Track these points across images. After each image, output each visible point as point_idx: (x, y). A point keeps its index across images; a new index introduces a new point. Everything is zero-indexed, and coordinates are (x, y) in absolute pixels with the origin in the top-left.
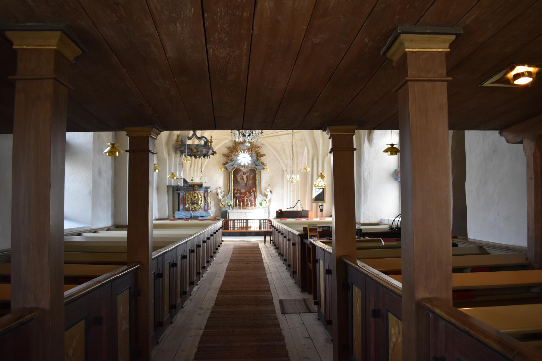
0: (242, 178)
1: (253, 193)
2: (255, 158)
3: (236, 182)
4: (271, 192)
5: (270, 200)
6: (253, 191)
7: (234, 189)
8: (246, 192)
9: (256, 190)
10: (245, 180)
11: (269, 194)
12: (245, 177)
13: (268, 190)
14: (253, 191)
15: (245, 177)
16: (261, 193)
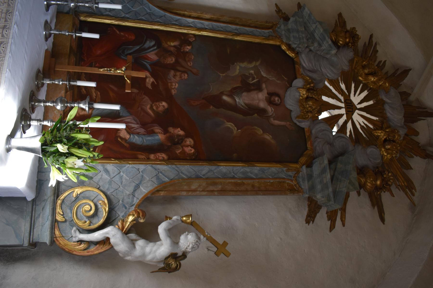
0: (246, 86)
1: (160, 137)
2: (362, 161)
3: (224, 52)
4: (173, 263)
5: (103, 258)
6: (176, 142)
7: (184, 39)
8: (169, 98)
9: (185, 158)
10: (241, 100)
11: (161, 249)
12: (259, 99)
13: (187, 241)
14: (176, 142)
15: (259, 99)
16: (163, 197)
